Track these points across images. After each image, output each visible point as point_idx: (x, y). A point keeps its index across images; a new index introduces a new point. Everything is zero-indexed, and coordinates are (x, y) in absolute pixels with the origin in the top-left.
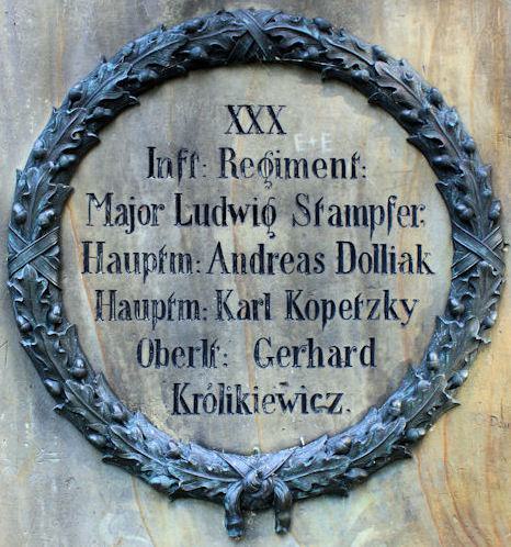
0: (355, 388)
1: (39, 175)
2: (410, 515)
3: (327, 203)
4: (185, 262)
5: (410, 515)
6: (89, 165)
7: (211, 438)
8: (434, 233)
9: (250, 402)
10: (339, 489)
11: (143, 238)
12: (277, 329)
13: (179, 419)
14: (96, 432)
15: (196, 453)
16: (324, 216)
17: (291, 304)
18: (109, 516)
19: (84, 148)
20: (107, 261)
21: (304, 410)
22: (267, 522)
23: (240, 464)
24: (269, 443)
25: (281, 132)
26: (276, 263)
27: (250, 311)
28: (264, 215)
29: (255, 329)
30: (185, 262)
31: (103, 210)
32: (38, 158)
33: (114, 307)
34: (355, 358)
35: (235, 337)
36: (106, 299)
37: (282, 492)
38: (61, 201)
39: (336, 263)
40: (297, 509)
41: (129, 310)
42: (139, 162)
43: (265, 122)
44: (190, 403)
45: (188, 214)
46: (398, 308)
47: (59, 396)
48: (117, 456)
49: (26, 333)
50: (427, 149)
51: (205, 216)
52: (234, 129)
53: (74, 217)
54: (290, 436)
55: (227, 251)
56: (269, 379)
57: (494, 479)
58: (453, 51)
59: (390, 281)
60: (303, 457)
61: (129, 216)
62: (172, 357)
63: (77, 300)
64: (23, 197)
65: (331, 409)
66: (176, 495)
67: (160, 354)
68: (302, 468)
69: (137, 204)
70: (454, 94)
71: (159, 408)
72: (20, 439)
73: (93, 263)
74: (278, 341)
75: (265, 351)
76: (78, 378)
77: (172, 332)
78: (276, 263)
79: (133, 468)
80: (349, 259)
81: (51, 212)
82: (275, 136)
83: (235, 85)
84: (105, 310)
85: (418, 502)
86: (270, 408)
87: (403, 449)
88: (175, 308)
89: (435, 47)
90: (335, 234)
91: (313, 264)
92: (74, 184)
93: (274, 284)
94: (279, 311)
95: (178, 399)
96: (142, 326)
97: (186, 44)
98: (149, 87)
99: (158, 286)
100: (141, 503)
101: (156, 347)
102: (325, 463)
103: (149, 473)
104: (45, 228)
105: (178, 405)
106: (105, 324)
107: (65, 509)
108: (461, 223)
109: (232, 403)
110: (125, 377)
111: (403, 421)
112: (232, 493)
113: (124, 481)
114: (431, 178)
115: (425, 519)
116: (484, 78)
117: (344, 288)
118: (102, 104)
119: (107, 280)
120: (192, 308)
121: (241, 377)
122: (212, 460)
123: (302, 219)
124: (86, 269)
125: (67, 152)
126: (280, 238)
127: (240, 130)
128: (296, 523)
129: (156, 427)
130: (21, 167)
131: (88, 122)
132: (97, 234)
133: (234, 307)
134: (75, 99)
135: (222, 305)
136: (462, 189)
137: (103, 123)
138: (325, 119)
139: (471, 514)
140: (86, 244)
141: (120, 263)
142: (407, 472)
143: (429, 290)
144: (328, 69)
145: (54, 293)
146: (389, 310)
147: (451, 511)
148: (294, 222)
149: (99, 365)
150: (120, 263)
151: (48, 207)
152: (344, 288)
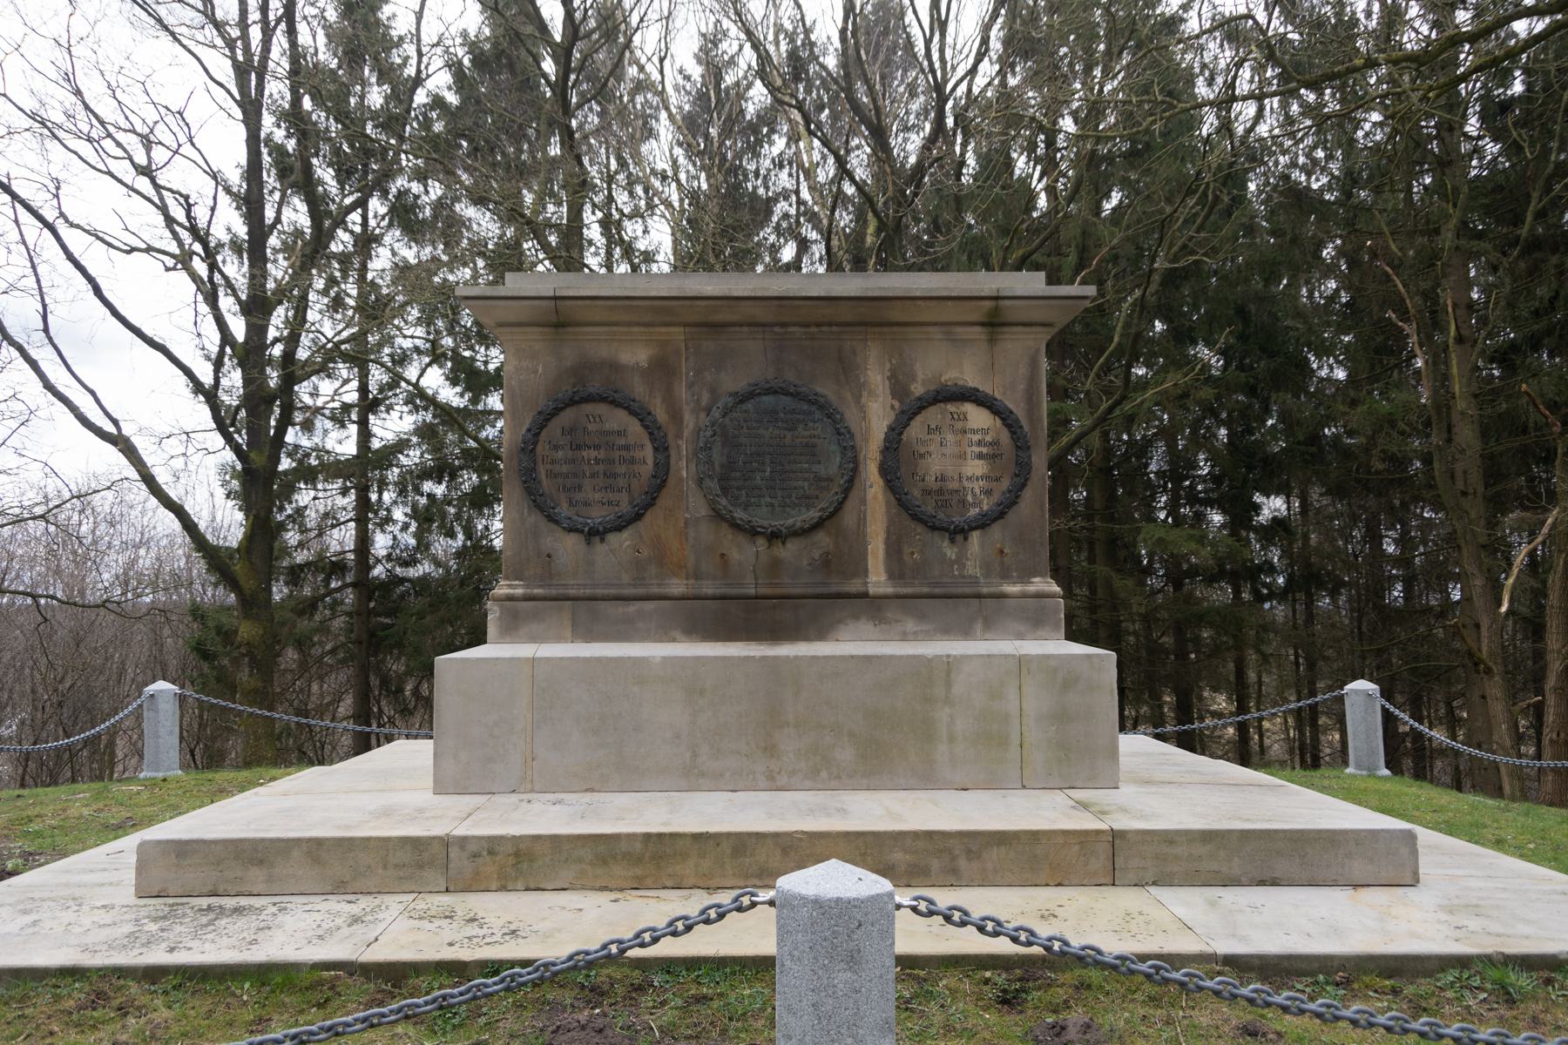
0: (624, 498)
1: (529, 435)
4: (573, 461)
8: (648, 453)
10: (619, 529)
11: (560, 453)
19: (542, 428)
22: (597, 539)
27: (593, 476)
30: (573, 461)
32: (529, 430)
33: (551, 475)
38: (535, 443)
42: (559, 431)
48: (552, 519)
50: (646, 427)
51: (579, 447)
56: (597, 496)
59: (635, 467)
61: (556, 448)
66: (570, 530)
71: (565, 505)
79: (557, 522)
83: (588, 408)
87: (638, 517)
90: (617, 453)
93: (600, 468)
96: (560, 480)
98: (562, 409)
99: (565, 469)
100: (560, 533)
108: (656, 449)
109: (586, 504)
113: (554, 526)
117: (622, 469)
120: (575, 475)
126: (602, 454)
129: (564, 510)
137: (548, 420)
138: (617, 419)
141: (553, 462)
143: (648, 468)
144: (614, 403)
150: (553, 462)
152: (622, 469)
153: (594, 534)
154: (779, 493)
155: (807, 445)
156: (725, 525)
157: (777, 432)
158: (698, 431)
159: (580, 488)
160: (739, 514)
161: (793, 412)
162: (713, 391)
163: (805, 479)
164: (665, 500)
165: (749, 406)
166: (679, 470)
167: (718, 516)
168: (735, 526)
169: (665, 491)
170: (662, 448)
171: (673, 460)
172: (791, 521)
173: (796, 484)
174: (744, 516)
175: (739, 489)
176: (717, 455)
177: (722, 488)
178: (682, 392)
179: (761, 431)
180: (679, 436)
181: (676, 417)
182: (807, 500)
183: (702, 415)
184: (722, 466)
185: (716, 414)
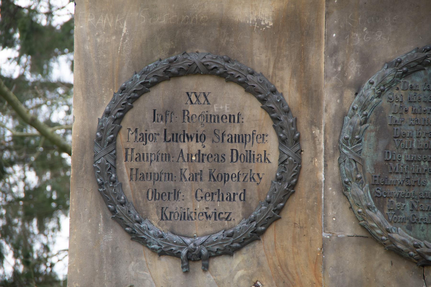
0: (237, 209)
1: (108, 121)
2: (259, 264)
3: (227, 133)
4: (167, 157)
5: (259, 264)
6: (128, 116)
7: (176, 230)
9: (193, 215)
10: (229, 252)
11: (150, 146)
12: (204, 185)
13: (163, 222)
14: (128, 226)
15: (169, 236)
16: (226, 138)
17: (211, 175)
18: (133, 263)
19: (125, 111)
20: (135, 156)
21: (215, 219)
22: (198, 266)
23: (188, 241)
24: (200, 232)
25: (209, 104)
26: (205, 158)
27: (194, 177)
28: (201, 138)
29: (196, 185)
30: (167, 157)
31: (134, 136)
32: (108, 114)
33: (138, 175)
34: (237, 198)
35: (187, 188)
36: (134, 172)
37: (204, 252)
38: (116, 132)
39: (230, 158)
40: (211, 260)
41: (143, 177)
42: (149, 116)
43: (202, 99)
44: (168, 217)
45: (169, 137)
46: (256, 177)
47: (113, 212)
48: (137, 237)
49: (101, 185)
50: (269, 110)
51: (176, 138)
52: (189, 102)
53: (121, 138)
54: (209, 230)
55: (185, 153)
56: (200, 206)
57: (296, 250)
58: (282, 69)
59: (253, 166)
60: (214, 238)
61: (145, 138)
62: (161, 196)
63: (122, 173)
64: (101, 130)
65: (226, 219)
66: (162, 253)
67: (158, 196)
68: (213, 242)
69: (148, 133)
70: (282, 87)
71: (155, 218)
72: (97, 230)
73: (129, 157)
74: (205, 190)
75: (200, 194)
76: (122, 204)
77: (161, 186)
78: (205, 158)
80: (236, 156)
81: (112, 136)
82: (206, 105)
83: (189, 83)
84: (134, 177)
85: (263, 259)
86: (201, 218)
87: (256, 236)
88: (163, 176)
89: (274, 67)
90: (229, 146)
91: (221, 158)
92: (122, 124)
93: (205, 167)
94: (206, 178)
95: (163, 214)
96: (149, 183)
97: (169, 67)
98: (154, 84)
99: (156, 167)
100: (147, 257)
101: (154, 192)
102: (222, 240)
103: (150, 243)
104: (110, 143)
105: (163, 217)
106: (134, 183)
107: (115, 259)
108: (282, 141)
109: (185, 216)
110: (142, 204)
111: (254, 224)
112: (184, 252)
113: (138, 247)
114: (270, 123)
115: (266, 266)
116: (295, 81)
117: (234, 169)
118: (135, 92)
119: (135, 164)
120: (170, 176)
121: (190, 205)
122: (176, 238)
123: (216, 140)
124: (126, 160)
125: (119, 111)
126: (207, 148)
127: (192, 103)
128: (211, 267)
129: (153, 225)
130: (100, 117)
131: (128, 99)
132: (131, 145)
133: (187, 176)
134: (123, 90)
135: (182, 175)
136: (282, 128)
137: (134, 99)
138: (229, 99)
139: (286, 265)
140: (127, 149)
141: (140, 157)
142: (258, 247)
143: (270, 168)
144: (226, 77)
145: (113, 169)
146: (252, 178)
147: (277, 263)
148: (213, 141)
149: (131, 199)
150: (140, 157)
151: (112, 134)
152: (234, 169)
153: (195, 259)
156: (379, 251)
158: (341, 117)
159: (176, 194)
162: (365, 60)
164: (293, 213)
166: (314, 170)
167: (369, 236)
169: (294, 201)
170: (290, 140)
171: (306, 156)
174: (409, 238)
175: (400, 198)
176: (370, 151)
177: (376, 197)
178: (320, 60)
180: (315, 122)
181: (311, 96)
183: (349, 94)
184: (376, 166)
185: (368, 91)
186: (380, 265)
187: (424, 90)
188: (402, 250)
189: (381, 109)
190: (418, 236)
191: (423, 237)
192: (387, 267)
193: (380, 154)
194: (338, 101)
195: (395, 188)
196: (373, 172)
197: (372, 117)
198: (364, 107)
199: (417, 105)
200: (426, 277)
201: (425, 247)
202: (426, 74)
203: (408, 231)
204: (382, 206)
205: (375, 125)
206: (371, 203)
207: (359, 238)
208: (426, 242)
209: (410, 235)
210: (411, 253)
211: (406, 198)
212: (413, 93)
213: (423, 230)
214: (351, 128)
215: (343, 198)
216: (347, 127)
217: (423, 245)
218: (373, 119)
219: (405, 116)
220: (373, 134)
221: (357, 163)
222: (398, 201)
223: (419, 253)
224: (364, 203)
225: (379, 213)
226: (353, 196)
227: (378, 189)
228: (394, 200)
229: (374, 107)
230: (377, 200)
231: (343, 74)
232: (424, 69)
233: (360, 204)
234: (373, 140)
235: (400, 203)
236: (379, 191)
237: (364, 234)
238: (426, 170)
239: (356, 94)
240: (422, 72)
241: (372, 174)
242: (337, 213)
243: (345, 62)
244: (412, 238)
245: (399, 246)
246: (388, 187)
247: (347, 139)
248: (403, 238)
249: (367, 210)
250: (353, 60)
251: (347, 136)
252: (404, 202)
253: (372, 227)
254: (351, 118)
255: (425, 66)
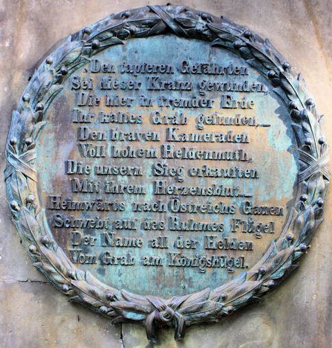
154: (172, 238)
155: (229, 139)
156: (62, 301)
157: (170, 112)
160: (90, 281)
161: (203, 69)
162: (42, 30)
163: (228, 211)
165: (111, 57)
167: (48, 284)
168: (78, 303)
172: (193, 299)
173: (207, 220)
175: (89, 228)
177: (57, 226)
179: (135, 110)
182: (228, 255)
183: (19, 77)
185: (46, 76)
186: (63, 321)
187: (123, 73)
188: (91, 305)
189: (63, 99)
190: (113, 282)
191: (119, 284)
192: (72, 324)
193: (62, 165)
194: (6, 89)
195: (82, 215)
196: (52, 191)
197: (50, 112)
198: (38, 96)
199: (111, 94)
200: (124, 337)
201: (123, 299)
202: (124, 50)
203: (99, 276)
204: (63, 240)
205: (55, 122)
206: (49, 236)
207: (35, 284)
208: (124, 291)
209: (102, 281)
210: (104, 308)
211: (98, 229)
212: (106, 76)
213: (120, 275)
214: (20, 126)
215: (11, 228)
216: (16, 127)
217: (119, 297)
218: (52, 115)
219: (96, 111)
220: (52, 136)
221: (28, 179)
222: (86, 233)
223: (114, 309)
224: (38, 237)
225: (60, 250)
226: (23, 226)
227: (58, 216)
228: (80, 232)
229: (53, 96)
230: (57, 232)
231: (13, 51)
232: (122, 44)
233: (32, 239)
234: (51, 144)
235: (88, 236)
236: (59, 219)
237: (40, 279)
238: (125, 188)
239: (30, 79)
240: (120, 47)
241: (51, 194)
242: (4, 249)
243: (16, 34)
244: (105, 286)
245: (88, 299)
246: (73, 212)
247: (12, 143)
248: (92, 288)
249: (42, 248)
250: (27, 31)
251: (15, 139)
252: (95, 235)
253: (49, 272)
254: (20, 113)
255: (123, 39)
